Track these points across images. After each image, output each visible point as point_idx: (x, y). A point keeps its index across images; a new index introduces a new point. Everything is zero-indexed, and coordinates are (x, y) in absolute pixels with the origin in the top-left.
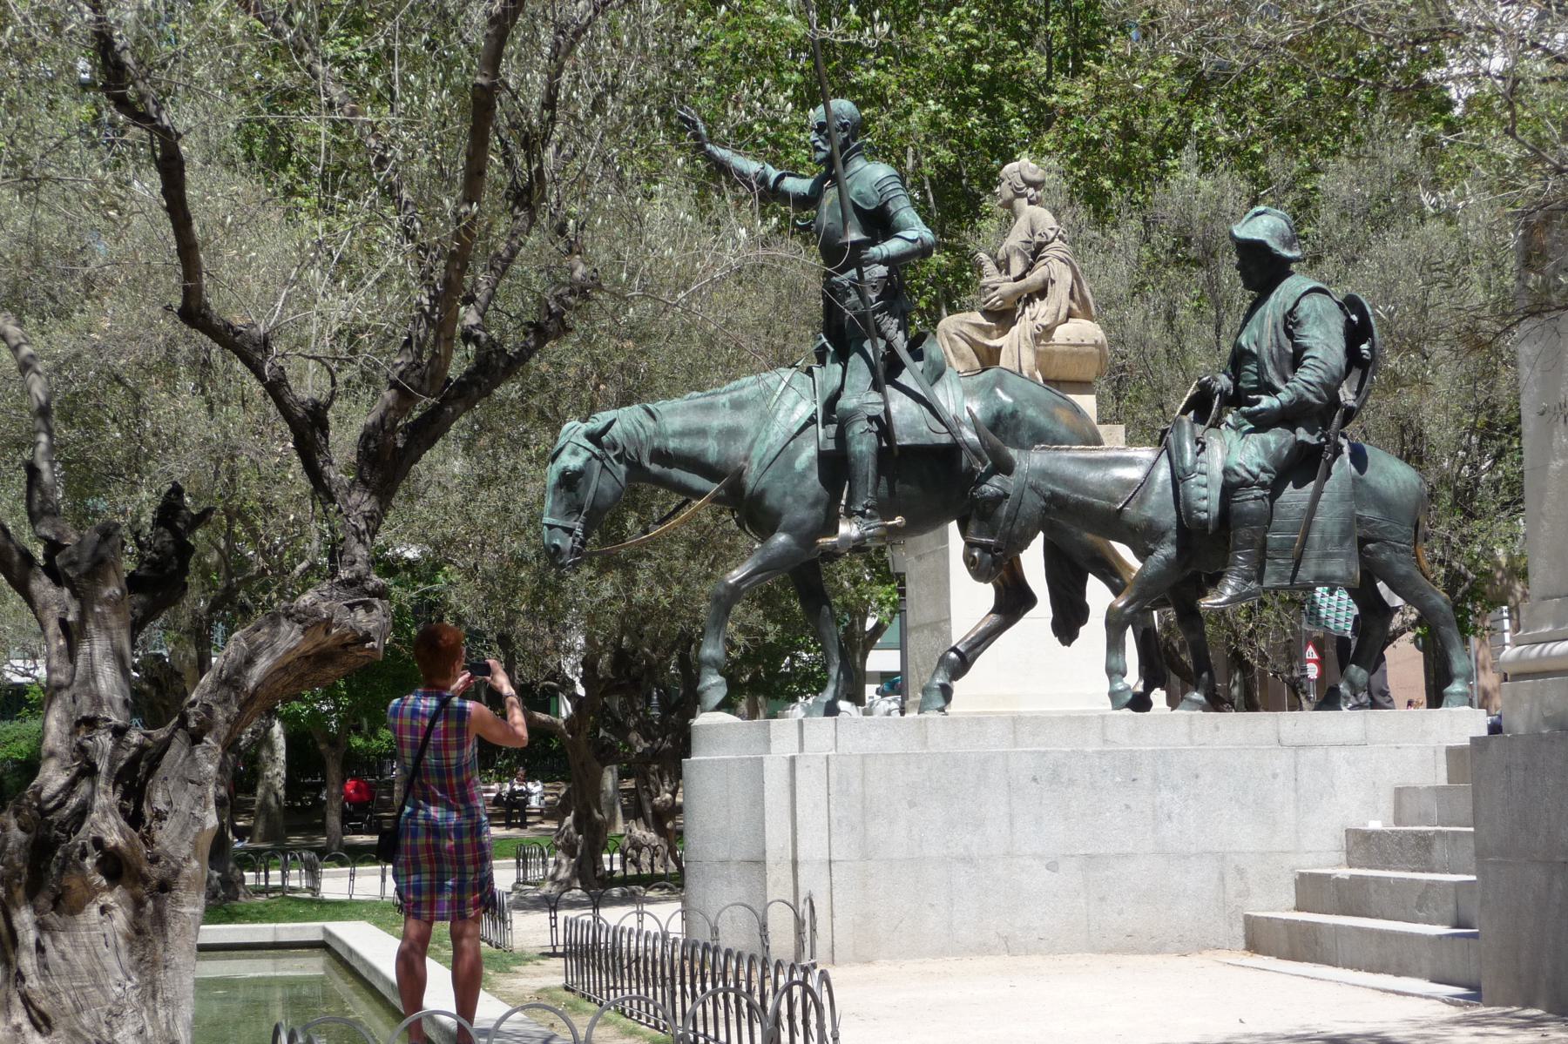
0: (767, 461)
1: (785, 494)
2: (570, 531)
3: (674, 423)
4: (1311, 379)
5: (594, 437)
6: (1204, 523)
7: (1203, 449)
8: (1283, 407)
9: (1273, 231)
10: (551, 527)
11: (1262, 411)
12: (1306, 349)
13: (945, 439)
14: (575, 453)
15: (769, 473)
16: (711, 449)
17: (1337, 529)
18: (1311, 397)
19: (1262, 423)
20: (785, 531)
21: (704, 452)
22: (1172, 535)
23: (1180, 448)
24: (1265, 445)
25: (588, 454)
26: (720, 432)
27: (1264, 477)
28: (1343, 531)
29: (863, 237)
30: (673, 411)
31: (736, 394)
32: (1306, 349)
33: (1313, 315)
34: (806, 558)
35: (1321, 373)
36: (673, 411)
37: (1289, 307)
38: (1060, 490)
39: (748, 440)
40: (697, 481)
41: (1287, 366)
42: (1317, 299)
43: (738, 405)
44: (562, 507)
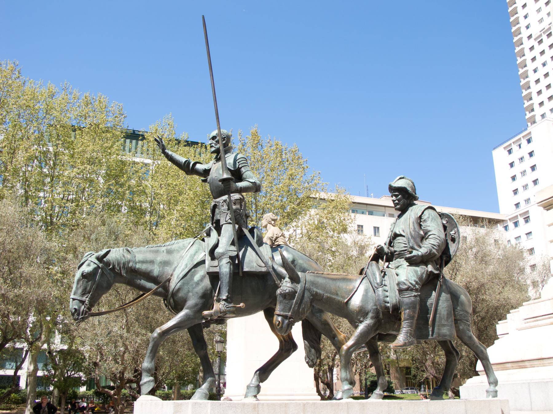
0: (181, 276)
1: (189, 292)
2: (83, 302)
3: (139, 257)
4: (435, 243)
6: (387, 308)
7: (385, 274)
8: (422, 256)
9: (408, 184)
10: (74, 299)
11: (414, 256)
12: (429, 231)
13: (264, 270)
14: (89, 265)
15: (182, 281)
16: (156, 271)
17: (445, 313)
18: (434, 251)
19: (413, 262)
21: (151, 271)
23: (374, 274)
24: (416, 272)
25: (96, 266)
26: (161, 262)
27: (417, 286)
28: (448, 314)
29: (230, 176)
30: (140, 251)
31: (169, 247)
32: (429, 231)
33: (431, 217)
34: (197, 322)
35: (438, 241)
37: (419, 214)
38: (320, 291)
39: (174, 267)
40: (149, 285)
41: (418, 240)
42: (430, 211)
43: (169, 252)
44: (80, 291)
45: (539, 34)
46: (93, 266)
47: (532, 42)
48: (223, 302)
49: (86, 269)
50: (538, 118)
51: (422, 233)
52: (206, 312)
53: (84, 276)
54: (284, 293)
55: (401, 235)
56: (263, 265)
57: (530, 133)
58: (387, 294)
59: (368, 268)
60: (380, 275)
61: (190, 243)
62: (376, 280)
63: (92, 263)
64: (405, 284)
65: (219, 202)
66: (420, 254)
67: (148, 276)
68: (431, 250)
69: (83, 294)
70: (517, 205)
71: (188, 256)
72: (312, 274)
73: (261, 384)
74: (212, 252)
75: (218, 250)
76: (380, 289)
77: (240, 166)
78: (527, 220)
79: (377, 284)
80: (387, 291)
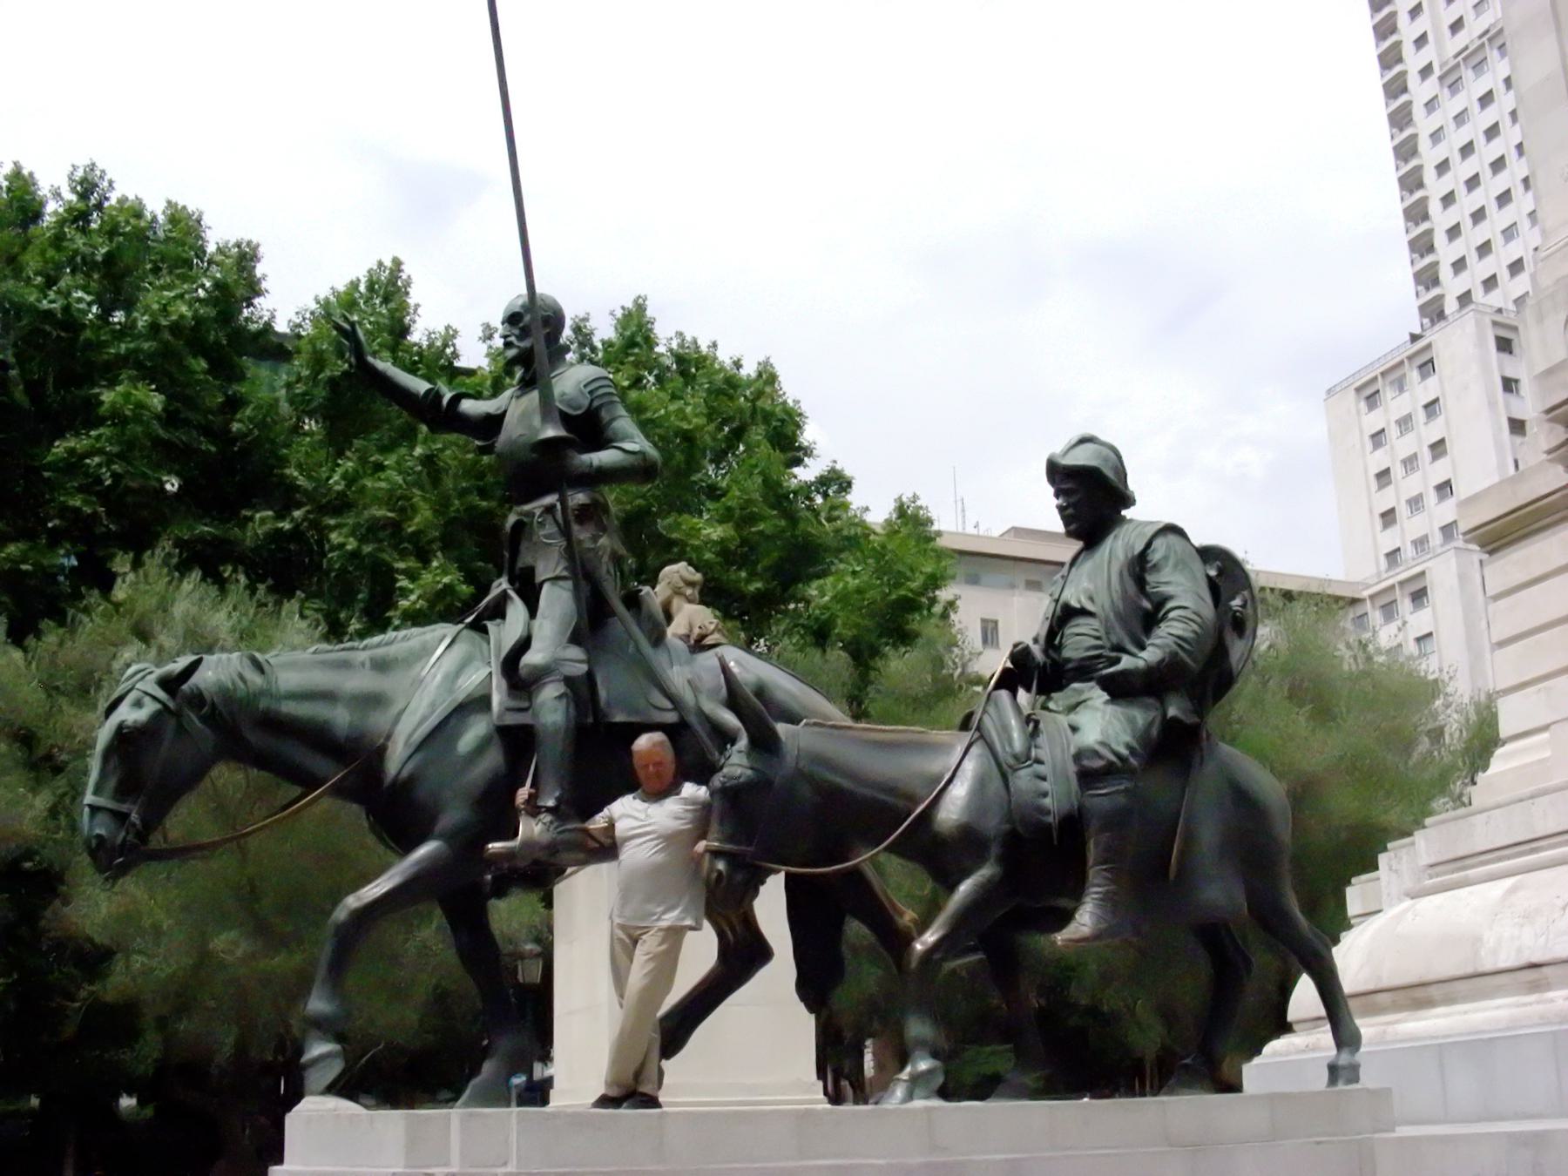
3: (288, 680)
5: (170, 684)
10: (94, 809)
14: (138, 704)
19: (1121, 689)
20: (440, 837)
22: (995, 850)
23: (1005, 729)
24: (1131, 721)
31: (380, 651)
35: (1195, 627)
36: (293, 665)
37: (1139, 548)
40: (317, 763)
42: (1172, 539)
44: (112, 783)
45: (1453, 63)
46: (150, 708)
47: (1431, 87)
48: (547, 818)
49: (128, 714)
50: (1451, 306)
51: (1147, 605)
52: (495, 846)
53: (124, 736)
54: (731, 788)
55: (1083, 612)
56: (669, 705)
57: (1429, 346)
58: (1045, 786)
59: (985, 711)
60: (1023, 731)
61: (444, 637)
62: (1011, 745)
63: (147, 699)
64: (1096, 754)
65: (530, 514)
66: (1141, 664)
67: (317, 737)
68: (1174, 655)
69: (122, 793)
70: (1393, 555)
71: (439, 678)
72: (816, 729)
73: (664, 1063)
74: (511, 664)
75: (533, 658)
76: (1022, 773)
77: (596, 404)
78: (1419, 596)
79: (1016, 757)
80: (1044, 779)
